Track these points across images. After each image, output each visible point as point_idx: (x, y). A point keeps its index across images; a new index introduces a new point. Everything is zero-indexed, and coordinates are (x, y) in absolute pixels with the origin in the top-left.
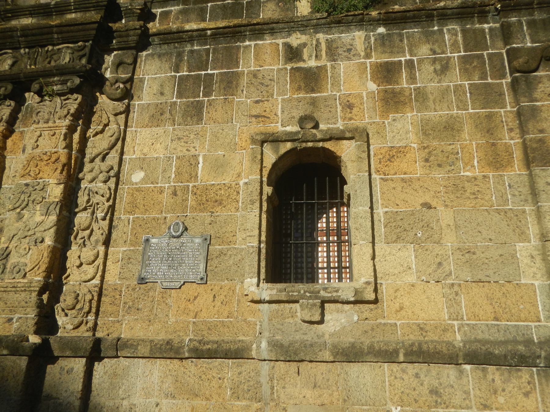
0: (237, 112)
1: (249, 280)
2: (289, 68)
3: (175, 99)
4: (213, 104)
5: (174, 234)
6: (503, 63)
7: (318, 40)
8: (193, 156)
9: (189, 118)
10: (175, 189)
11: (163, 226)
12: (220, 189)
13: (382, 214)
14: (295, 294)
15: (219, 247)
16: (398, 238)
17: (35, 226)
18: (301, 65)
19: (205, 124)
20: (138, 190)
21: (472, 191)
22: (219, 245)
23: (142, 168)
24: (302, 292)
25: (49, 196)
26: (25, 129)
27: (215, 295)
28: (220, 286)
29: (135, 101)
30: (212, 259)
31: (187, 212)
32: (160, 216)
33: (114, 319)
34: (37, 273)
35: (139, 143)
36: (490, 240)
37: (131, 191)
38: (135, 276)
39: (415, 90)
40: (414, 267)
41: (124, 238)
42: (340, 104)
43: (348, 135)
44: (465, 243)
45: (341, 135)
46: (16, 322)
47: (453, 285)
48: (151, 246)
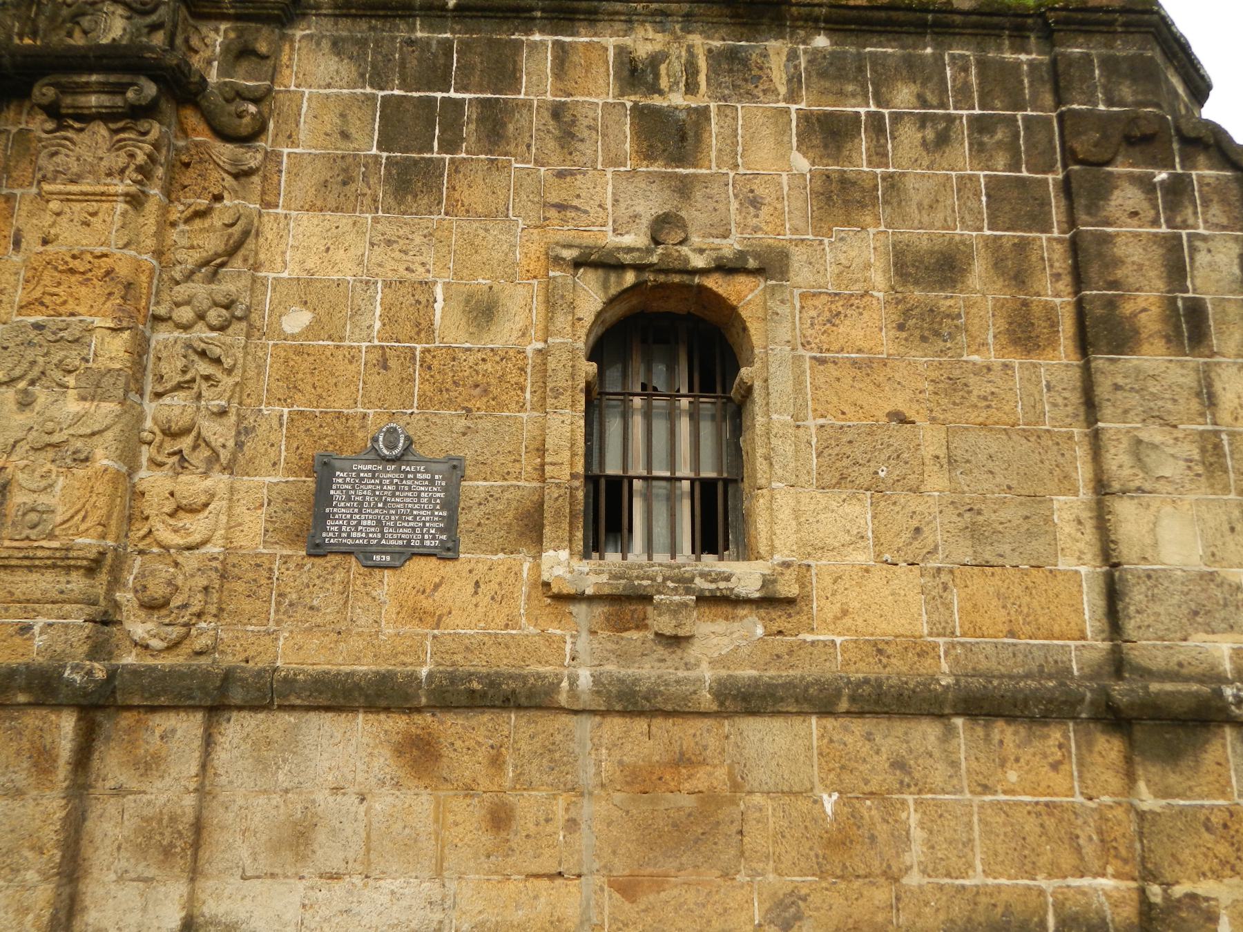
0: (516, 193)
1: (551, 553)
2: (629, 105)
3: (374, 151)
4: (462, 169)
5: (386, 452)
6: (1051, 140)
7: (690, 49)
8: (421, 283)
9: (409, 198)
10: (384, 354)
12: (483, 360)
13: (813, 430)
14: (645, 583)
16: (843, 477)
17: (69, 422)
18: (657, 101)
19: (447, 214)
20: (299, 351)
21: (982, 393)
22: (485, 479)
23: (306, 303)
24: (660, 579)
25: (95, 355)
26: (18, 192)
27: (477, 583)
28: (489, 563)
29: (281, 146)
33: (256, 629)
34: (83, 527)
35: (296, 244)
36: (1009, 488)
37: (283, 354)
39: (884, 179)
40: (870, 534)
41: (272, 455)
42: (736, 196)
43: (752, 263)
44: (964, 493)
45: (739, 264)
46: (41, 634)
47: (939, 570)
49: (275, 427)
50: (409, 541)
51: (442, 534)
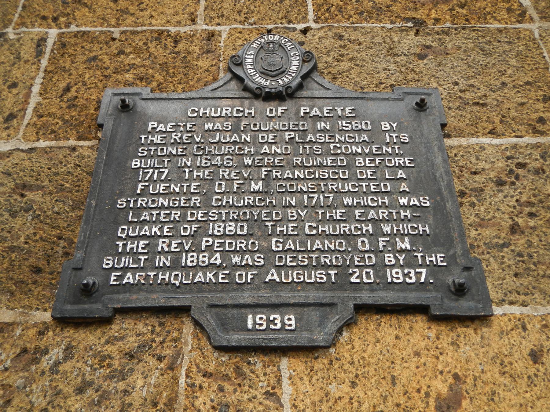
11: (204, 63)
15: (497, 141)
22: (492, 133)
31: (305, 19)
32: (182, 29)
49: (25, 55)
51: (428, 250)
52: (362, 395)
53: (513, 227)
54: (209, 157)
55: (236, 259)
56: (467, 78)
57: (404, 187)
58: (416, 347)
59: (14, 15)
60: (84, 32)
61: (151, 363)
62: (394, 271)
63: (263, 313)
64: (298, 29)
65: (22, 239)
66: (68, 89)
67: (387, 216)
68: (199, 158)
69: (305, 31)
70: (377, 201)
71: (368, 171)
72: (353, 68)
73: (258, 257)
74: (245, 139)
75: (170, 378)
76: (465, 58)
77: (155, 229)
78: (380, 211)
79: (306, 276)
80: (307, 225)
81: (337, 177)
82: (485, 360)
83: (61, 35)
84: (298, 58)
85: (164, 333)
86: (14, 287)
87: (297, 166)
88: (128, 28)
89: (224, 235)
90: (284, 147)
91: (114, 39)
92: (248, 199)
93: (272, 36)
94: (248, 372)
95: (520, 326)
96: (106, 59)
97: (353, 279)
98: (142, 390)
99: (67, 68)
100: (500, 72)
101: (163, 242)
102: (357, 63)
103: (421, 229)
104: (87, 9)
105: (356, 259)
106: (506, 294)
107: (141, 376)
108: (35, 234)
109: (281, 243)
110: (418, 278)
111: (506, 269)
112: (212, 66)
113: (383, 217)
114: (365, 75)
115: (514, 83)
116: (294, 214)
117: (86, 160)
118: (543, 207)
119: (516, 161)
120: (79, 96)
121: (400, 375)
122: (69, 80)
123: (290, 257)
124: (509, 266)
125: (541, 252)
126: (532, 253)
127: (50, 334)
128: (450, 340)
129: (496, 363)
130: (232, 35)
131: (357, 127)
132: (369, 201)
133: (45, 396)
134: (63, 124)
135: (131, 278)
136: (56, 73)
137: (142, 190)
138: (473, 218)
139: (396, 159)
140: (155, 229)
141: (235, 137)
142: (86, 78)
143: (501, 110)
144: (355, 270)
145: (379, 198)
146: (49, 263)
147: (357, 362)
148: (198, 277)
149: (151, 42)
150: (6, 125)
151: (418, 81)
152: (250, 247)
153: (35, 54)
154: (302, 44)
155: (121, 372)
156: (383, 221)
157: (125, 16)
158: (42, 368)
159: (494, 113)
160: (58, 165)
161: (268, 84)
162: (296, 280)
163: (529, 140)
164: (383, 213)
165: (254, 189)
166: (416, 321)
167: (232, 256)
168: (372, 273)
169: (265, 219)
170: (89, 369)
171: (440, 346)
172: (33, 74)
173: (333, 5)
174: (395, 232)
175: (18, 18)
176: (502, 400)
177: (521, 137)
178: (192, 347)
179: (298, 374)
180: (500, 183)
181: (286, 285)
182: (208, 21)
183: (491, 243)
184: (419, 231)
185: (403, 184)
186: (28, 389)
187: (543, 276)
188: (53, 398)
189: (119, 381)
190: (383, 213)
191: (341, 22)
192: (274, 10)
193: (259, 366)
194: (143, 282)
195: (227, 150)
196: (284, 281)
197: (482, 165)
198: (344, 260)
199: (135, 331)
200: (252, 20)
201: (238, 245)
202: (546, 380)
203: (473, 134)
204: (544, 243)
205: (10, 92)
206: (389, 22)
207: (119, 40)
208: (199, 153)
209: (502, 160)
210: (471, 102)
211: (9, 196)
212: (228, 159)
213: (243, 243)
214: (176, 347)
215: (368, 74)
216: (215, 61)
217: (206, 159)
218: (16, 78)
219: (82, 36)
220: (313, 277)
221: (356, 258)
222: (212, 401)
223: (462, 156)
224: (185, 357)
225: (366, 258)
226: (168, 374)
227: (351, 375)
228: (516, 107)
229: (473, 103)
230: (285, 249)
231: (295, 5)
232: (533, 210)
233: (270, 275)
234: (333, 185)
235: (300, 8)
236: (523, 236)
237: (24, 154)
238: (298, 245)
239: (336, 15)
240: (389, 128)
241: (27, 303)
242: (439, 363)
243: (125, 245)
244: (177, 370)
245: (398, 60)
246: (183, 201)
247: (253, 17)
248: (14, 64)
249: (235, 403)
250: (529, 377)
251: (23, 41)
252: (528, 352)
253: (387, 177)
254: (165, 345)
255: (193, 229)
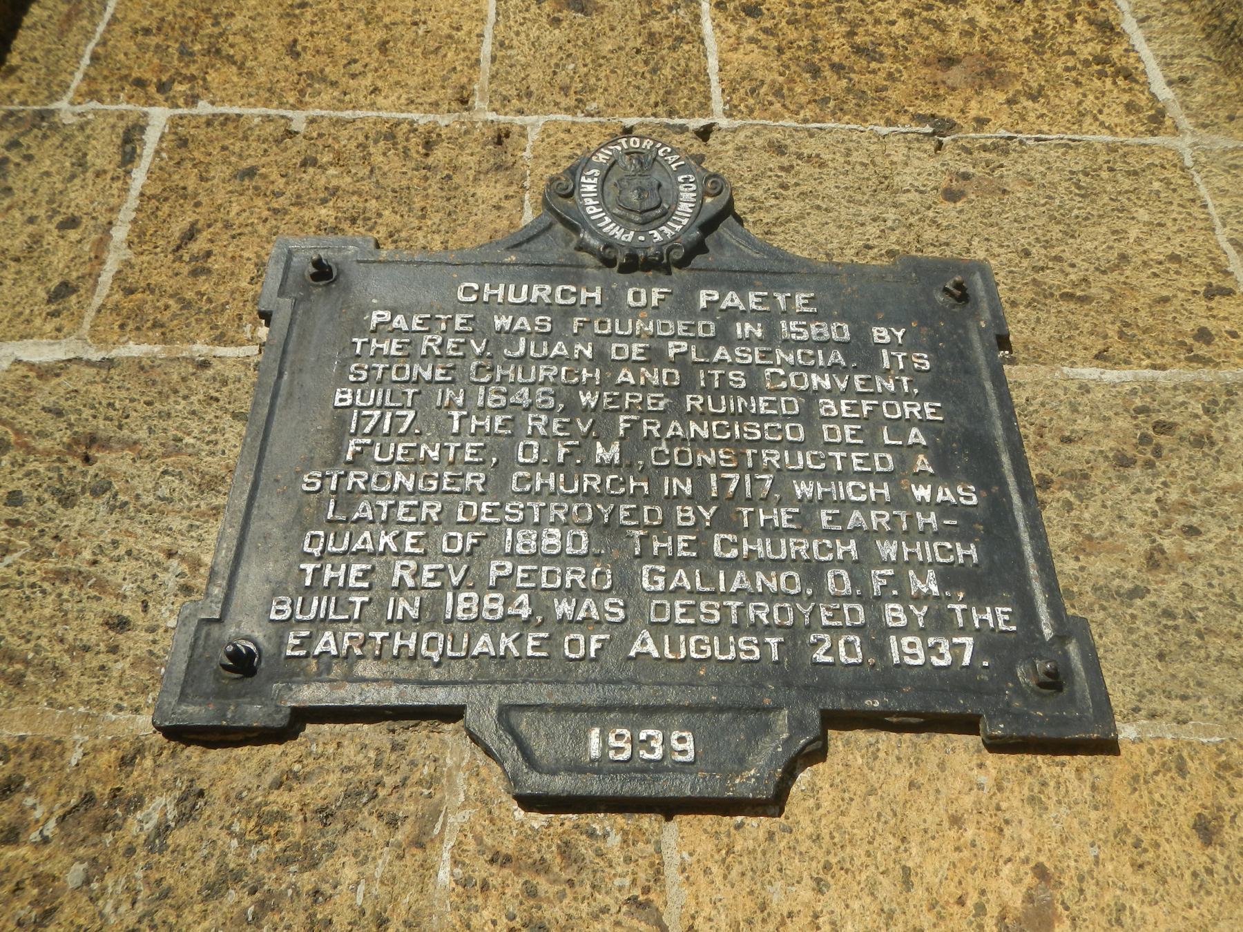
15: (1111, 375)
22: (1102, 357)
30: (1079, 478)
31: (705, 107)
32: (444, 120)
38: (136, 643)
48: (359, 327)
50: (794, 636)
52: (838, 908)
53: (1152, 554)
54: (504, 389)
55: (563, 608)
56: (1047, 241)
57: (923, 463)
58: (954, 807)
59: (72, 73)
60: (227, 118)
61: (375, 832)
62: (906, 640)
63: (623, 725)
64: (691, 129)
65: (87, 555)
66: (191, 235)
67: (888, 523)
68: (482, 390)
69: (704, 134)
70: (866, 491)
71: (846, 427)
72: (809, 214)
73: (611, 605)
74: (581, 352)
75: (417, 864)
76: (1043, 201)
77: (386, 539)
78: (873, 514)
79: (717, 647)
80: (717, 538)
81: (779, 438)
82: (1101, 836)
83: (175, 123)
84: (694, 187)
85: (404, 767)
86: (67, 658)
87: (693, 414)
88: (323, 112)
89: (536, 557)
90: (665, 372)
91: (291, 134)
92: (590, 481)
93: (638, 140)
94: (589, 855)
95: (1173, 765)
96: (274, 176)
97: (820, 656)
98: (355, 891)
99: (190, 189)
100: (1114, 232)
101: (403, 567)
102: (819, 202)
103: (960, 551)
104: (234, 69)
105: (824, 613)
106: (1141, 697)
107: (353, 860)
108: (115, 543)
109: (661, 574)
110: (957, 658)
111: (1142, 642)
112: (507, 197)
113: (879, 524)
114: (834, 230)
115: (1145, 257)
116: (690, 514)
117: (231, 386)
118: (1213, 515)
119: (1155, 417)
120: (216, 250)
121: (920, 867)
122: (195, 217)
123: (682, 606)
124: (1146, 637)
125: (1212, 609)
126: (1194, 610)
127: (148, 763)
128: (1026, 792)
129: (1125, 843)
130: (549, 136)
131: (820, 334)
132: (850, 491)
133: (134, 903)
134: (181, 309)
135: (332, 642)
136: (166, 199)
137: (355, 454)
138: (1067, 536)
139: (905, 403)
140: (386, 539)
141: (559, 349)
142: (233, 214)
143: (1121, 311)
144: (821, 636)
145: (871, 485)
146: (145, 607)
147: (827, 838)
148: (480, 643)
149: (376, 142)
150: (53, 307)
151: (947, 244)
152: (594, 581)
153: (118, 158)
154: (700, 159)
155: (307, 849)
156: (880, 533)
157: (317, 86)
158: (128, 838)
159: (1106, 317)
160: (168, 397)
161: (629, 240)
162: (694, 655)
163: (1181, 373)
164: (878, 516)
165: (602, 459)
166: (953, 750)
167: (556, 601)
168: (858, 643)
169: (626, 523)
170: (235, 843)
171: (1004, 805)
172: (114, 201)
173: (763, 82)
174: (906, 559)
175: (83, 80)
176: (1138, 923)
177: (1163, 368)
178: (467, 798)
179: (699, 861)
180: (1123, 462)
181: (674, 665)
182: (497, 105)
183: (1106, 586)
184: (957, 557)
185: (921, 457)
186: (95, 886)
187: (1219, 660)
188: (152, 906)
189: (303, 870)
190: (878, 516)
191: (783, 117)
192: (638, 88)
193: (615, 840)
194: (358, 652)
195: (542, 374)
196: (671, 656)
197: (1082, 423)
198: (797, 614)
199: (338, 762)
200: (592, 106)
201: (569, 578)
202: (1230, 881)
203: (1063, 359)
204: (1217, 590)
205: (62, 237)
206: (882, 122)
207: (305, 137)
208: (482, 380)
209: (1126, 415)
210: (1057, 293)
211: (59, 460)
212: (544, 393)
213: (578, 572)
214: (430, 796)
215: (840, 227)
216: (514, 187)
217: (497, 392)
218: (77, 206)
219: (223, 124)
220: (732, 648)
221: (822, 609)
222: (512, 918)
223: (1043, 405)
224: (451, 819)
225: (846, 612)
226: (413, 855)
227: (814, 864)
228: (1150, 307)
229: (1062, 296)
230: (672, 587)
231: (683, 80)
232: (1194, 520)
233: (638, 642)
234: (773, 455)
235: (695, 85)
236: (1173, 575)
237: (94, 371)
238: (698, 579)
239: (771, 103)
240: (888, 339)
241: (97, 695)
242: (1004, 841)
243: (318, 573)
244: (433, 848)
245: (903, 198)
246: (446, 481)
247: (594, 99)
248: (73, 177)
249: (563, 922)
250: (1195, 875)
251: (93, 129)
252: (1192, 822)
253: (887, 442)
254: (407, 793)
255: (470, 541)
